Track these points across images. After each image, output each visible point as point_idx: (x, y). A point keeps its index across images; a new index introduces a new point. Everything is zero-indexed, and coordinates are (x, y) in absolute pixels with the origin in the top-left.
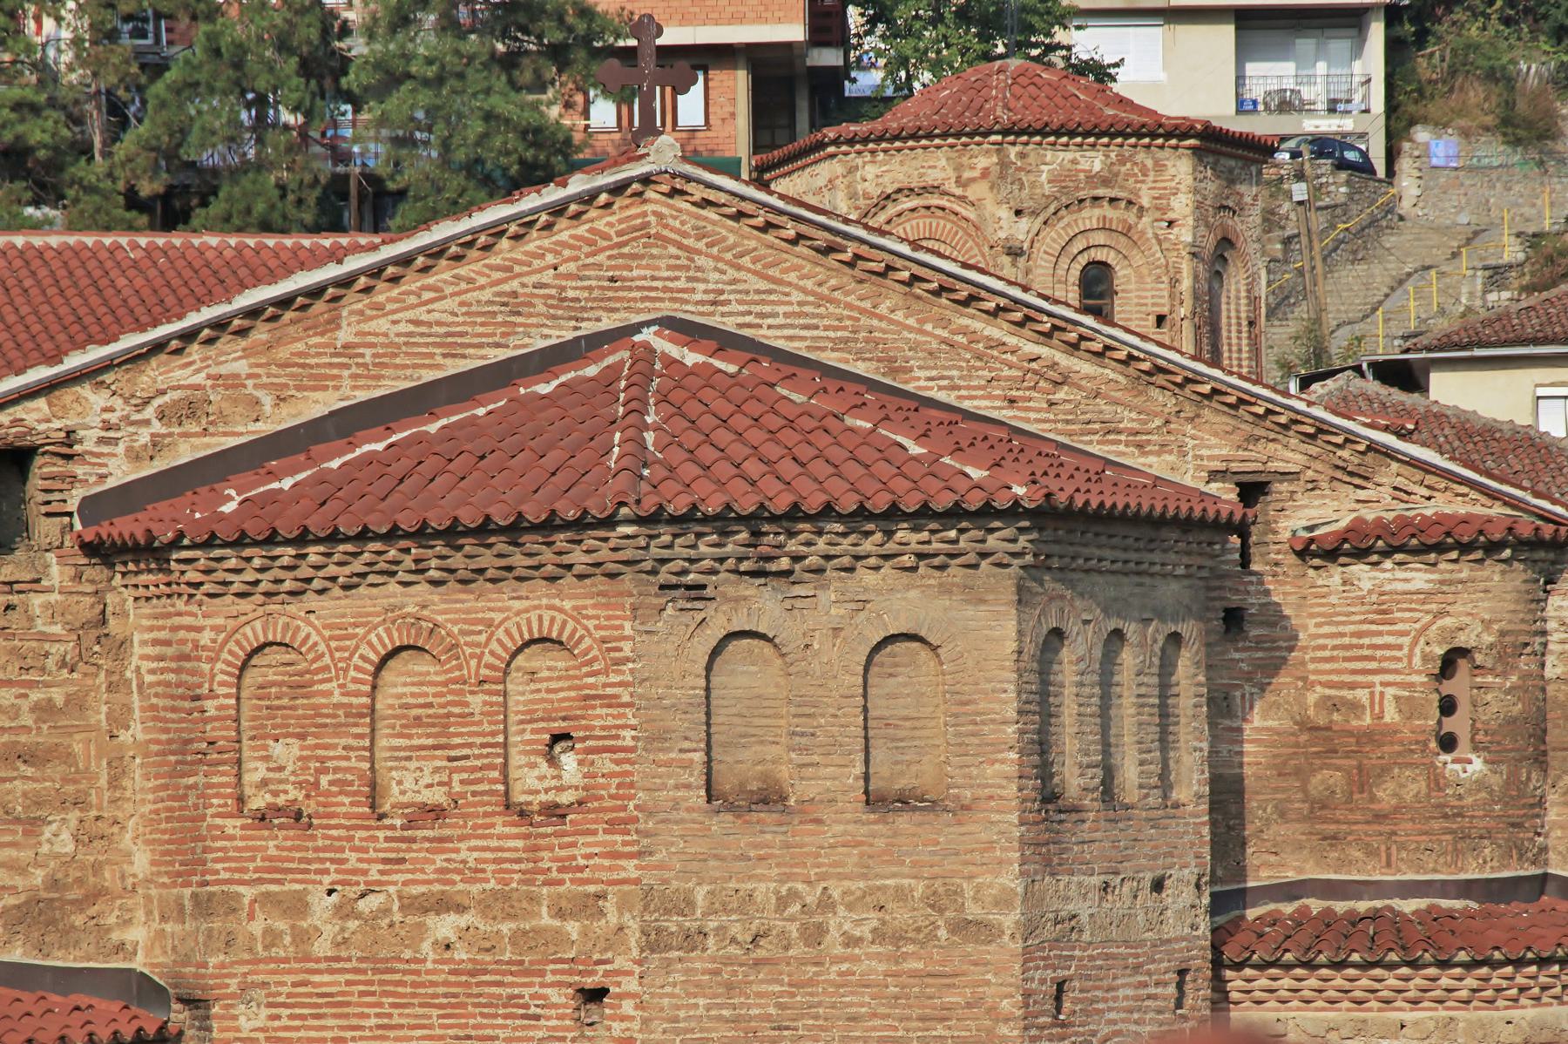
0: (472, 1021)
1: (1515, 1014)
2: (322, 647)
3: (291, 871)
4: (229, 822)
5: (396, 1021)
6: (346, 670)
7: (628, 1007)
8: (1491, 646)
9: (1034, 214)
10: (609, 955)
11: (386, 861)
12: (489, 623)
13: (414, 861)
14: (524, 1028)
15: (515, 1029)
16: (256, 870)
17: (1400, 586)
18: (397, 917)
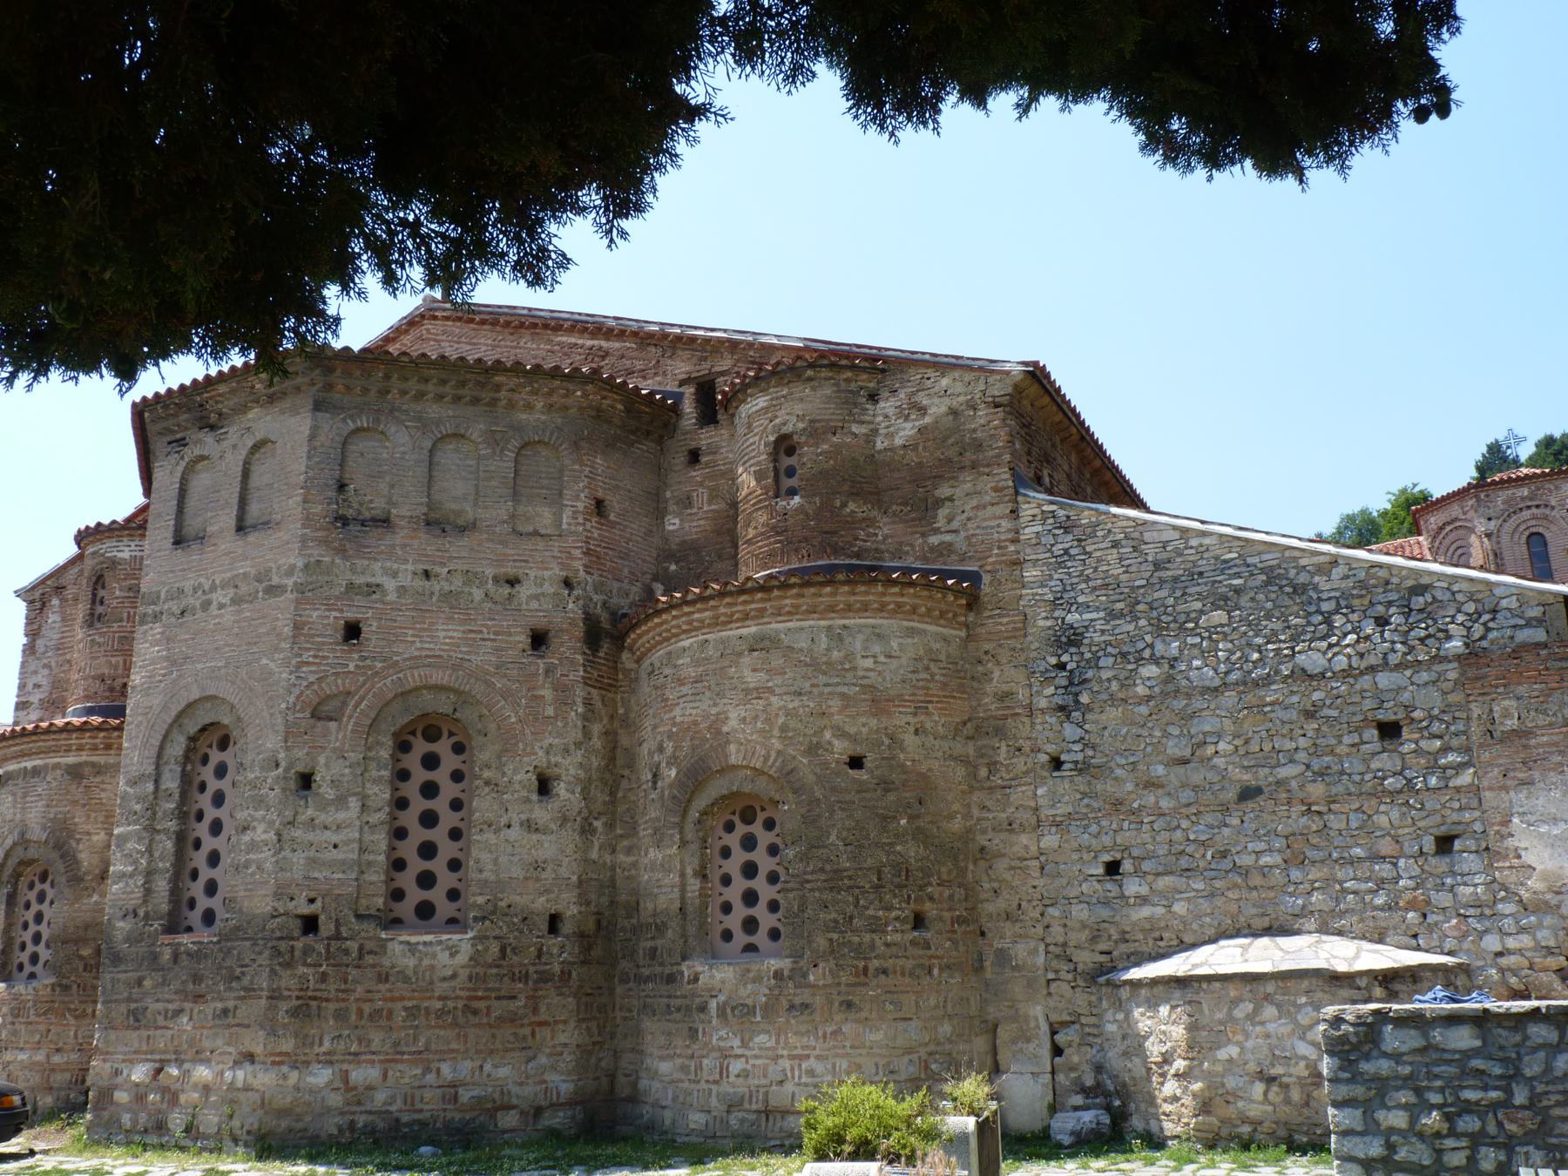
1: (744, 631)
8: (804, 429)
9: (1498, 518)
17: (754, 409)
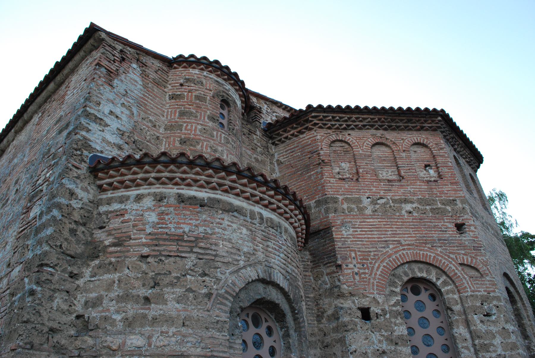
0: (424, 232)
2: (354, 141)
3: (354, 192)
4: (332, 179)
5: (398, 232)
6: (363, 148)
7: (472, 228)
10: (462, 215)
11: (385, 190)
12: (403, 139)
13: (394, 190)
14: (442, 234)
15: (439, 234)
16: (342, 192)
18: (392, 205)
